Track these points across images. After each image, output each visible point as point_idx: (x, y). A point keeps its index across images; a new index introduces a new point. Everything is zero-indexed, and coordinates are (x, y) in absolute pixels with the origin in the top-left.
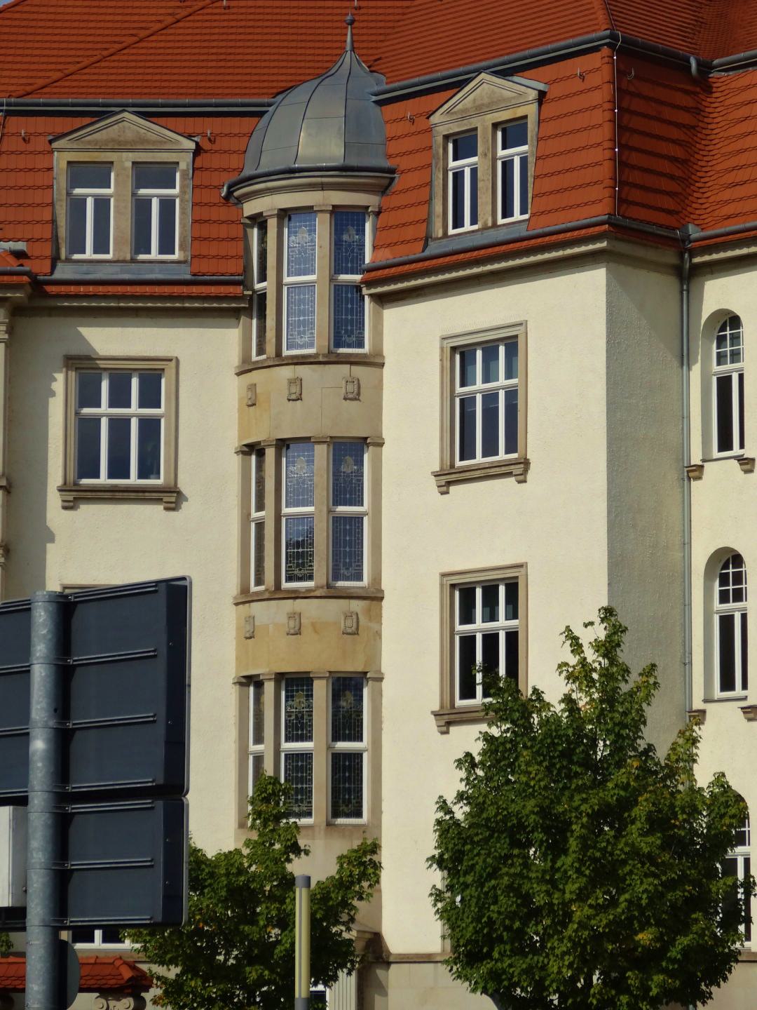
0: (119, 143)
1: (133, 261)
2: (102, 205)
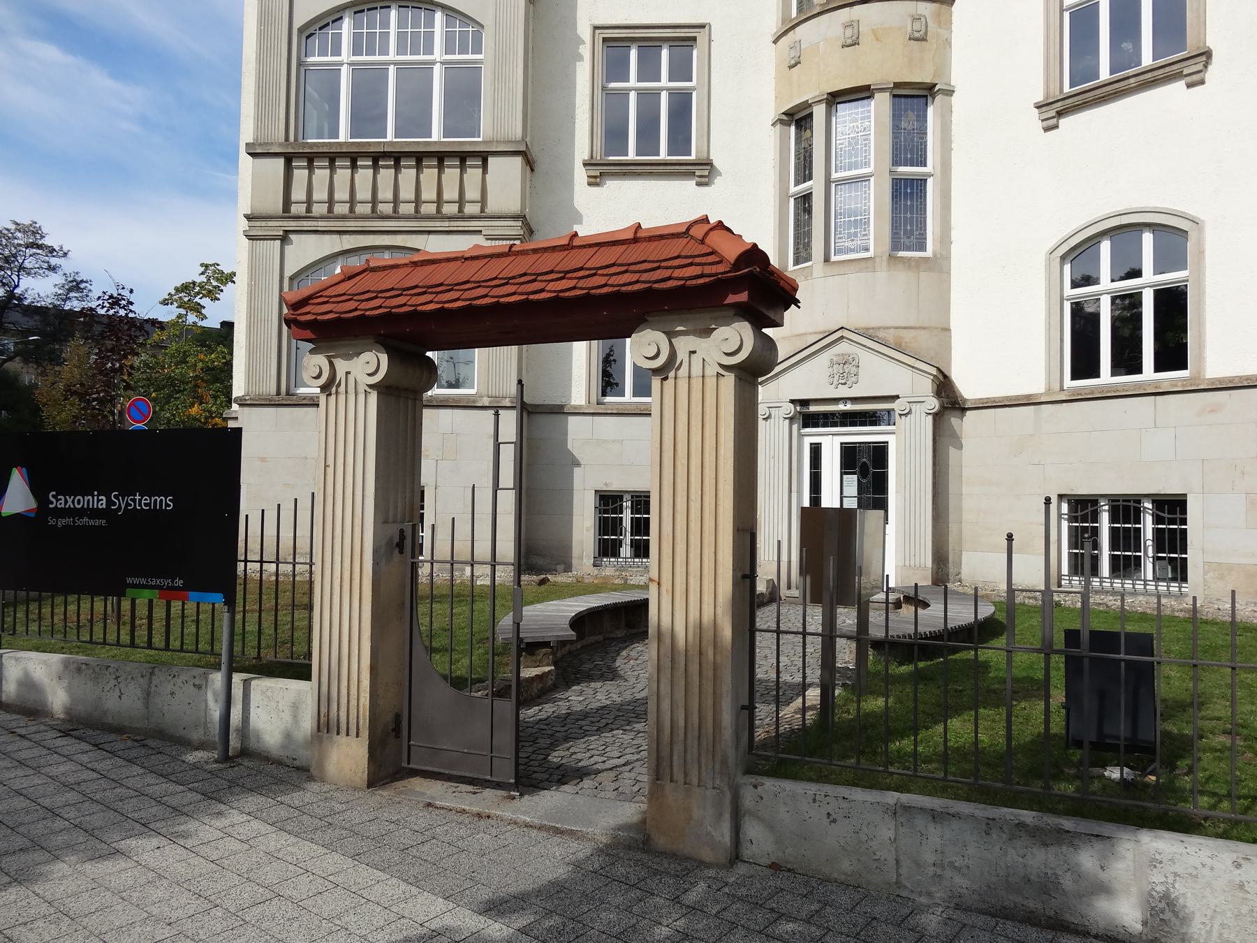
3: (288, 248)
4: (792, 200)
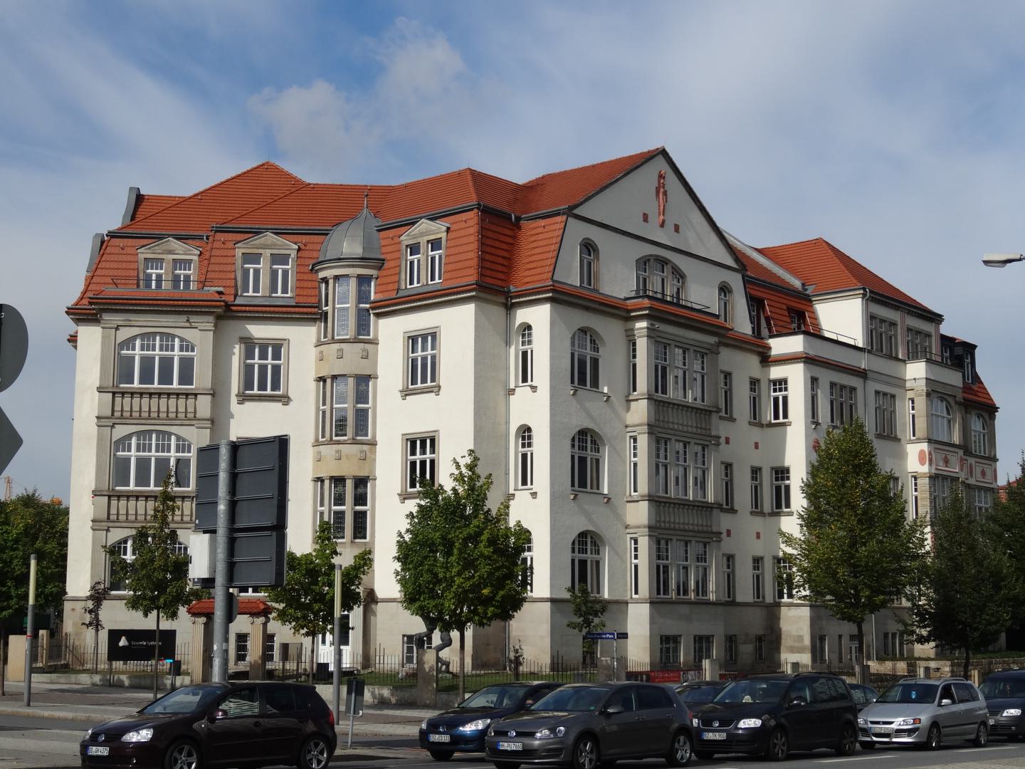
0: (265, 245)
1: (270, 296)
2: (257, 272)
4: (318, 513)
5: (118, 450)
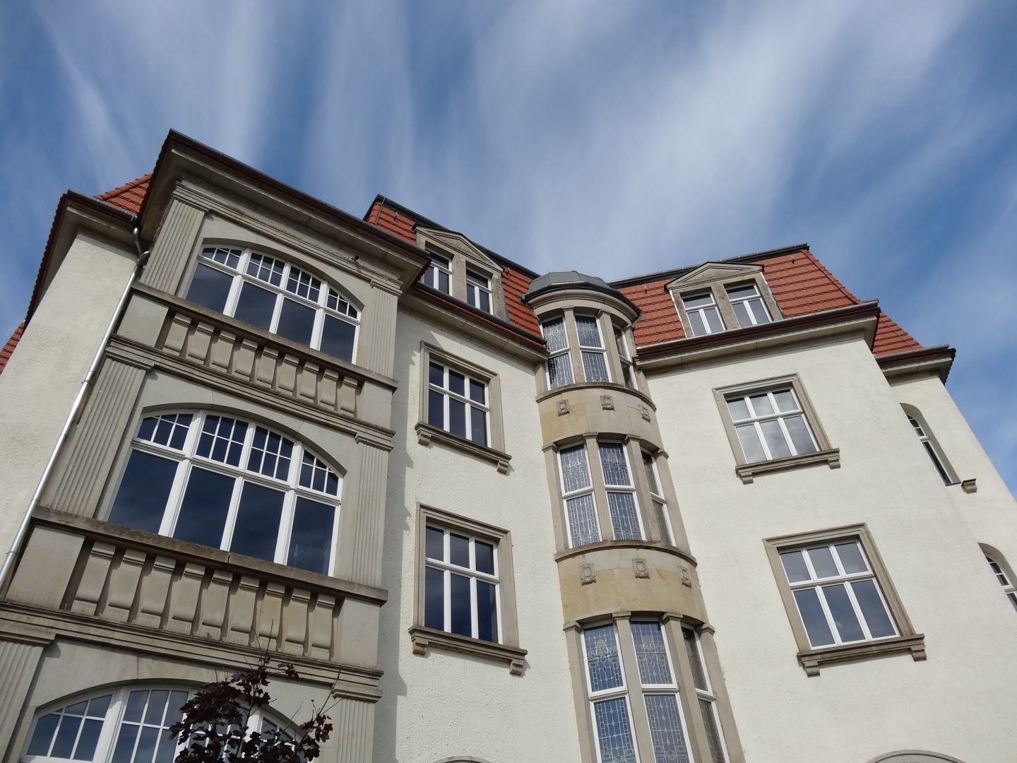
3: (50, 662)
5: (145, 433)
